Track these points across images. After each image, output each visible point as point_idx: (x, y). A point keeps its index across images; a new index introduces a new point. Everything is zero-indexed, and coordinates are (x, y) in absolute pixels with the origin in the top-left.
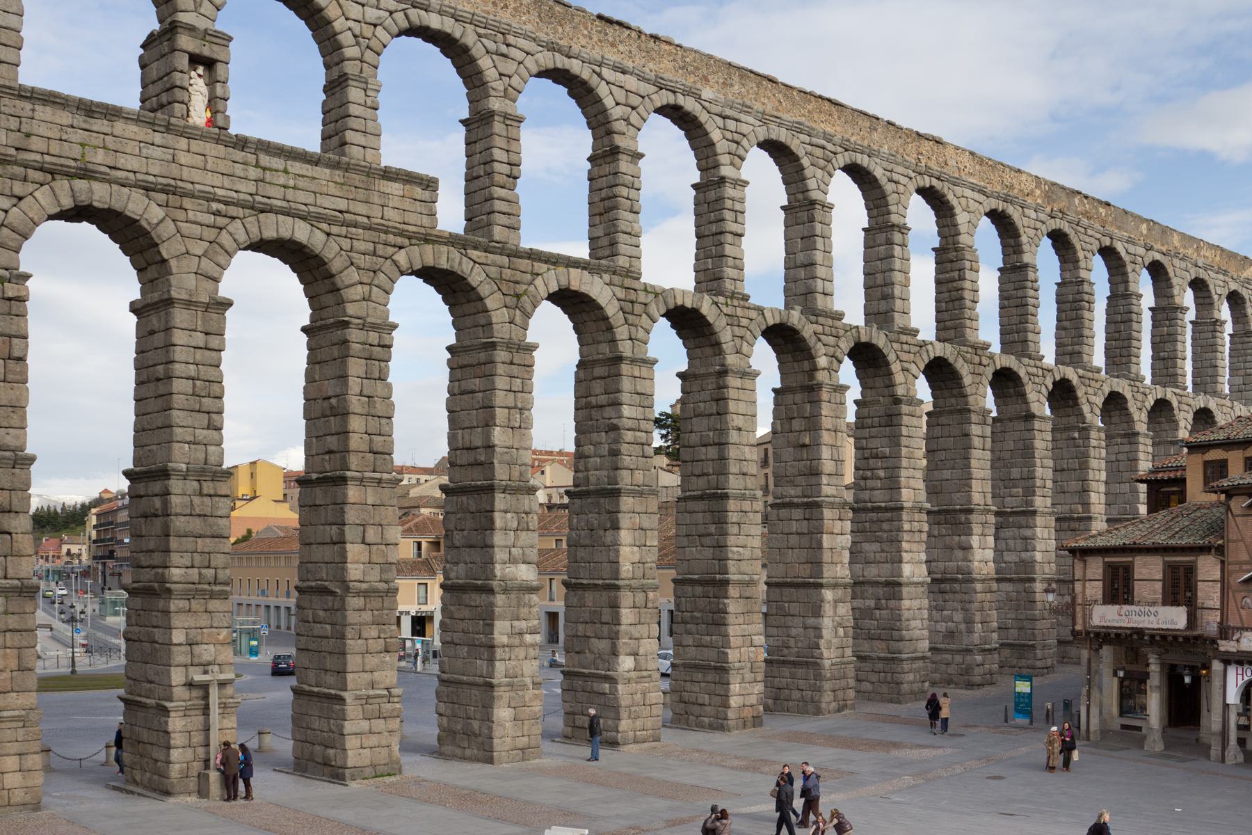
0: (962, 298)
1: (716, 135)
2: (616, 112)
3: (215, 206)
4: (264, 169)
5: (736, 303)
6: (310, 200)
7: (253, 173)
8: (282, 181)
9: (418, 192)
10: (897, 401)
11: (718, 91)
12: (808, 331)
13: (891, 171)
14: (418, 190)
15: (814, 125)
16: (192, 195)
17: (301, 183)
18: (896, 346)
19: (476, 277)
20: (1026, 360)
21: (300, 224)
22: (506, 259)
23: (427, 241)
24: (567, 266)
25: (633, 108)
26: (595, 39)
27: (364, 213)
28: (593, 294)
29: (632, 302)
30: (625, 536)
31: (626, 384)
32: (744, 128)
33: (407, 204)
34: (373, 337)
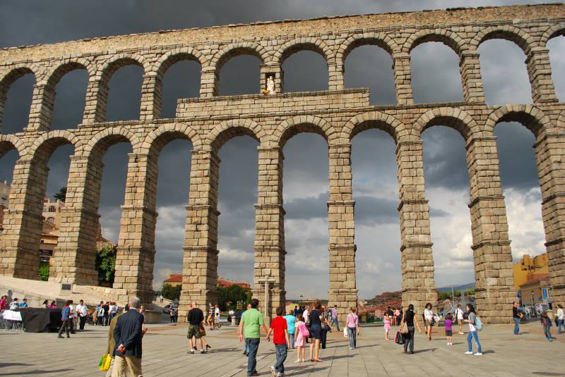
1: (525, 36)
3: (275, 118)
5: (549, 104)
6: (313, 107)
7: (291, 104)
9: (360, 95)
16: (267, 116)
21: (309, 117)
22: (405, 111)
23: (366, 111)
25: (472, 38)
26: (447, 18)
28: (455, 115)
29: (480, 115)
32: (544, 29)
33: (355, 100)
34: (340, 150)
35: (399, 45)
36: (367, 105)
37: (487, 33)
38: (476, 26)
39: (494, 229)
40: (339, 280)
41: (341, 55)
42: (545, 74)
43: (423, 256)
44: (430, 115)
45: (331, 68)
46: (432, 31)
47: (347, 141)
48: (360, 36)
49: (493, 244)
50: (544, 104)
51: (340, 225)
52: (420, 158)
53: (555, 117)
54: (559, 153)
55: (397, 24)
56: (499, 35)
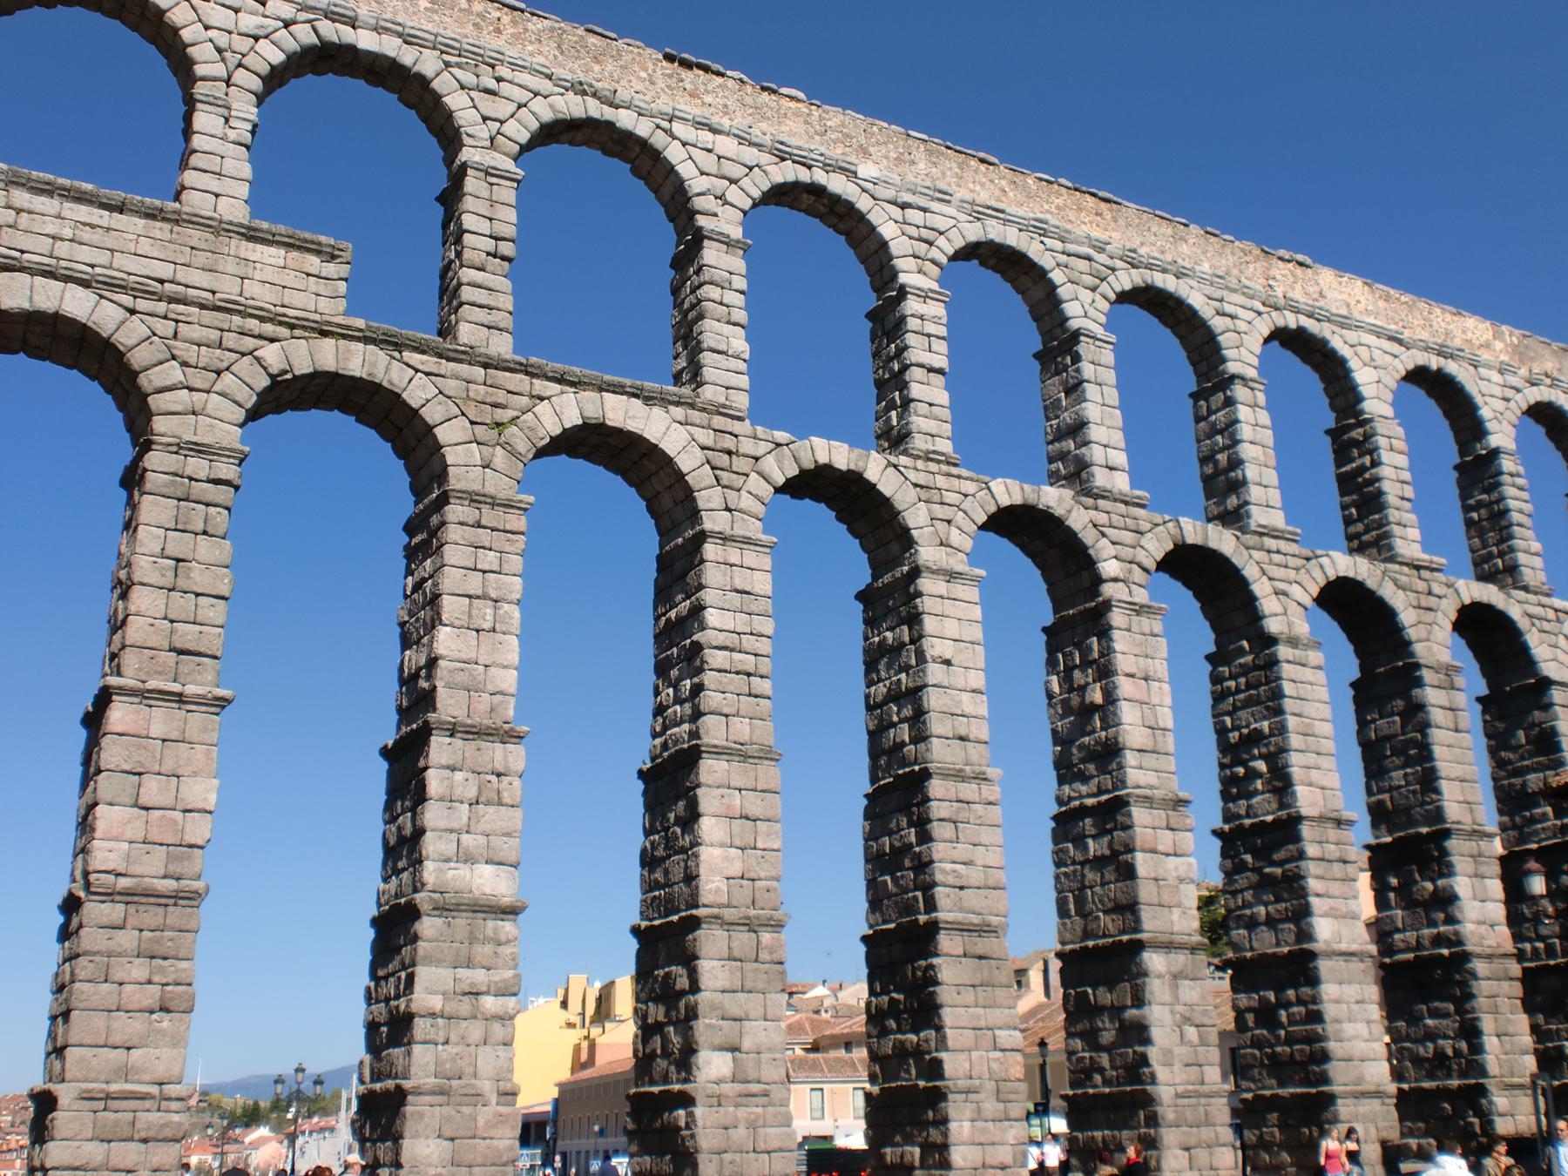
0: (1380, 493)
1: (887, 230)
2: (696, 184)
4: (19, 211)
5: (933, 467)
6: (102, 257)
8: (51, 228)
9: (313, 262)
10: (1272, 641)
11: (888, 168)
12: (1079, 519)
13: (1221, 300)
14: (315, 260)
15: (1069, 227)
17: (86, 234)
18: (1257, 555)
19: (417, 392)
20: (1521, 594)
22: (479, 372)
23: (324, 334)
24: (601, 390)
25: (733, 181)
26: (661, 84)
27: (205, 285)
29: (729, 453)
30: (709, 827)
31: (712, 575)
33: (289, 278)
34: (198, 466)
35: (485, 119)
36: (332, 310)
37: (780, 180)
38: (751, 144)
39: (736, 869)
40: (117, 1039)
41: (256, 84)
42: (931, 370)
43: (483, 951)
44: (565, 410)
45: (204, 119)
46: (608, 113)
47: (230, 435)
48: (347, 35)
49: (728, 925)
50: (920, 464)
51: (152, 790)
52: (516, 563)
53: (945, 512)
54: (948, 634)
55: (491, 42)
56: (807, 199)
